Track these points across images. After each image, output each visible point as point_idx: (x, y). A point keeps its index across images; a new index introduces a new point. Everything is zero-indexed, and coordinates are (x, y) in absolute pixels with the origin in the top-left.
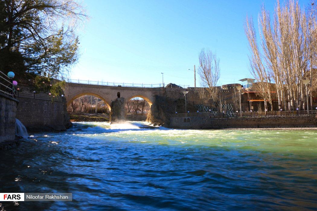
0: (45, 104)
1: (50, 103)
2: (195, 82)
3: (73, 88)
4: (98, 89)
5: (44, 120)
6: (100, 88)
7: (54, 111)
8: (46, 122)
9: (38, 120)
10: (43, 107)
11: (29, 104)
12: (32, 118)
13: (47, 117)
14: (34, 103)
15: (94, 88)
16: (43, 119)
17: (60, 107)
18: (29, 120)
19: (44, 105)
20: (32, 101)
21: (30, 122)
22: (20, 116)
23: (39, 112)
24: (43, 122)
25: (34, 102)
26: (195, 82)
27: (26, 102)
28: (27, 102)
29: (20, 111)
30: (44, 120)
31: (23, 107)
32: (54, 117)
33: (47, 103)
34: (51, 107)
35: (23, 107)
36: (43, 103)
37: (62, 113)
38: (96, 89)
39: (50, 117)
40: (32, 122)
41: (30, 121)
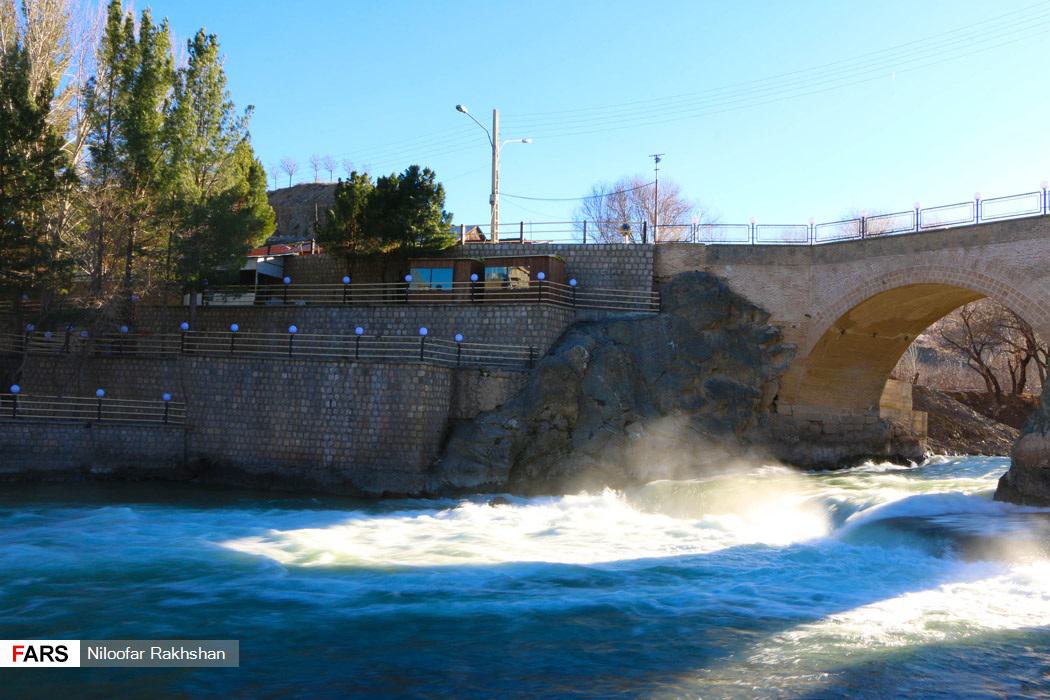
0: (331, 377)
1: (351, 371)
2: (494, 160)
3: (835, 270)
4: (974, 253)
5: (324, 444)
6: (987, 242)
7: (371, 406)
8: (333, 453)
9: (298, 441)
10: (323, 390)
11: (265, 381)
12: (277, 435)
13: (336, 429)
14: (285, 376)
15: (945, 252)
16: (323, 440)
17: (404, 387)
18: (266, 440)
19: (327, 380)
20: (276, 369)
21: (270, 448)
22: (232, 425)
23: (304, 410)
24: (319, 452)
25: (285, 371)
26: (494, 160)
27: (255, 374)
28: (259, 370)
29: (235, 406)
30: (324, 444)
31: (245, 392)
32: (371, 431)
33: (341, 372)
34: (357, 388)
35: (245, 392)
36: (322, 374)
37: (411, 415)
38: (961, 251)
39: (350, 430)
40: (277, 449)
41: (266, 445)
